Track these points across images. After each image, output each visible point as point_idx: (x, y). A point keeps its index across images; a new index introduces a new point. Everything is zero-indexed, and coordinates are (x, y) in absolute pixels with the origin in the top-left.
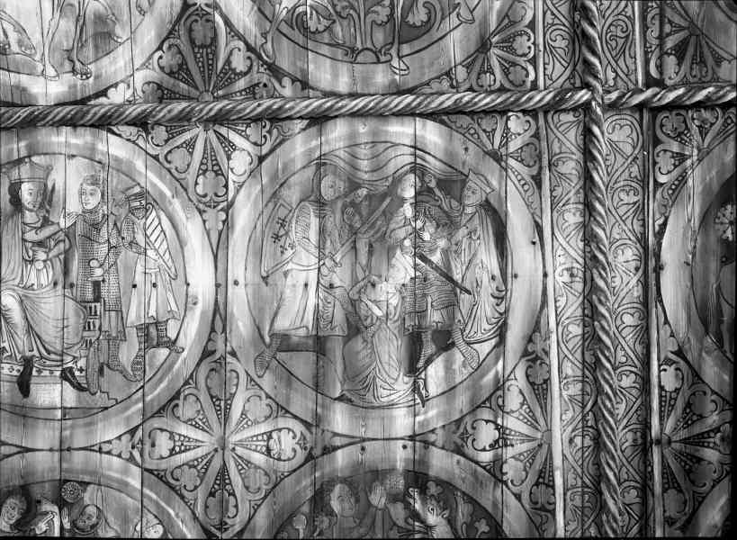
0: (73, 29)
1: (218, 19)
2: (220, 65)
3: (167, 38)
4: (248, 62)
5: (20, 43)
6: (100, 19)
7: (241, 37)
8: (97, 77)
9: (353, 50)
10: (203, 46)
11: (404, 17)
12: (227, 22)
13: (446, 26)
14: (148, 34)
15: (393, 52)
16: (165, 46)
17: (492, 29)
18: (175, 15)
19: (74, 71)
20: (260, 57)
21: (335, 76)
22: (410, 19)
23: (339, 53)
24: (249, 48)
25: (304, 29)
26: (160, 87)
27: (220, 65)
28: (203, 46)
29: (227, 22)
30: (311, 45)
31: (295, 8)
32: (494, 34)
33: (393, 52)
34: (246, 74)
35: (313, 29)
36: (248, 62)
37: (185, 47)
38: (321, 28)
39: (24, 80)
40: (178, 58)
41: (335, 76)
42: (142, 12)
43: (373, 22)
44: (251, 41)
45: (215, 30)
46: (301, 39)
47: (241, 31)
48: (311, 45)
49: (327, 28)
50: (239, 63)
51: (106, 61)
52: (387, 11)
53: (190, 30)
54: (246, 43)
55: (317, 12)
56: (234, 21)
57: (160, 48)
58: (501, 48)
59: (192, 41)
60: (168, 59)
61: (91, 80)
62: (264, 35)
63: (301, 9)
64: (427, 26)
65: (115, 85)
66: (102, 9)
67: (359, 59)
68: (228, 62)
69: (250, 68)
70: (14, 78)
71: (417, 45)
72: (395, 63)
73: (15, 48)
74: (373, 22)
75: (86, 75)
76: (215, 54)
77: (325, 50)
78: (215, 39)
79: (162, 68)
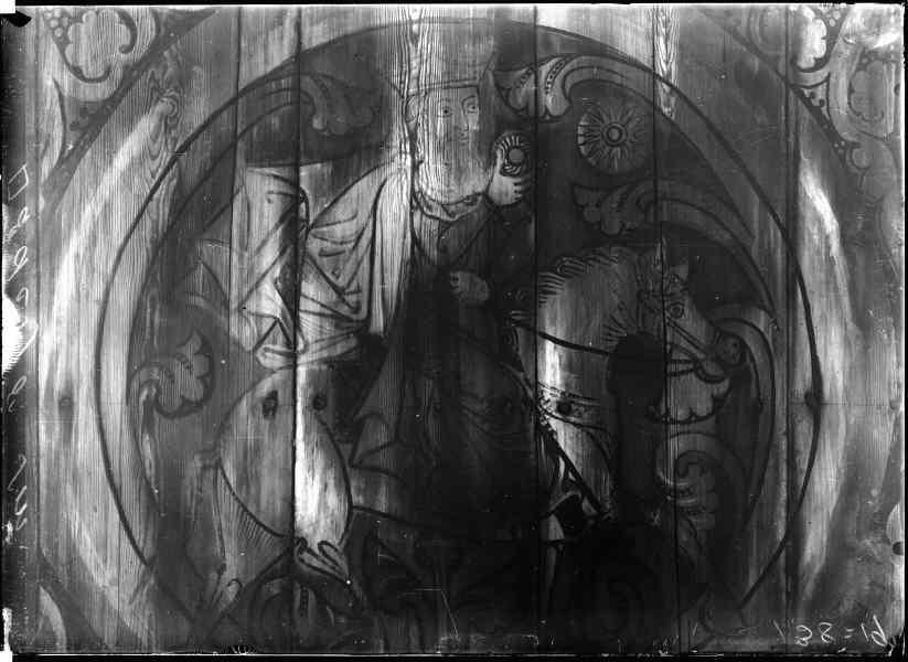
55: (318, 595)
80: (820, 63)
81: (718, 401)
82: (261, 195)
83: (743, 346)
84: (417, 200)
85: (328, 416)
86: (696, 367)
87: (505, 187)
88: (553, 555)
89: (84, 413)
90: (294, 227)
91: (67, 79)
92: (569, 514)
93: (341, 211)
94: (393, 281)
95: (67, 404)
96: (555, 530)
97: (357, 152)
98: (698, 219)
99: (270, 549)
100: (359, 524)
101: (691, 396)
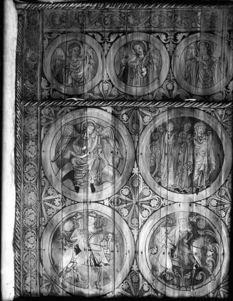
0: (97, 275)
1: (140, 275)
2: (140, 288)
3: (125, 280)
4: (148, 288)
5: (82, 279)
6: (106, 273)
7: (146, 281)
8: (104, 290)
9: (179, 286)
10: (135, 283)
11: (195, 277)
12: (143, 276)
13: (207, 281)
14: (119, 278)
15: (191, 288)
16: (124, 282)
17: (221, 282)
18: (127, 274)
19: (97, 288)
20: (151, 287)
21: (174, 293)
22: (196, 278)
23: (175, 287)
24: (149, 284)
25: (166, 280)
26: (122, 294)
27: (140, 288)
28: (135, 283)
29: (143, 276)
30: (167, 284)
31: (163, 273)
32: (221, 284)
33: (191, 288)
34: (147, 292)
35: (168, 279)
36: (148, 288)
37: (130, 284)
38: (170, 279)
39: (82, 290)
40: (127, 286)
41: (174, 293)
42: (118, 271)
43: (186, 278)
44: (149, 282)
45: (139, 279)
46: (164, 282)
47: (147, 279)
48: (167, 284)
49: (172, 279)
50: (146, 288)
51: (107, 286)
52: (190, 275)
53: (132, 278)
54: (148, 282)
56: (145, 276)
57: (123, 283)
58: (223, 288)
59: (132, 281)
60: (125, 286)
61: (102, 291)
62: (153, 280)
63: (165, 273)
64: (202, 281)
65: (109, 293)
66: (106, 271)
67: (181, 289)
68: (142, 288)
69: (149, 290)
70: (79, 289)
71: (198, 286)
72: (192, 291)
73: (80, 280)
74: (186, 278)
75: (101, 289)
76: (139, 285)
77: (171, 286)
78: (139, 281)
79: (123, 289)
80: (224, 217)
81: (213, 254)
82: (163, 230)
83: (215, 248)
84: (180, 231)
85: (170, 255)
86: (211, 251)
87: (189, 230)
88: (194, 271)
89: (144, 254)
90: (167, 233)
91: (142, 217)
92: (196, 266)
93: (171, 232)
94: (177, 240)
95: (142, 253)
96: (194, 268)
97: (173, 225)
98: (210, 234)
99: (164, 269)
100: (174, 267)
101: (210, 253)
